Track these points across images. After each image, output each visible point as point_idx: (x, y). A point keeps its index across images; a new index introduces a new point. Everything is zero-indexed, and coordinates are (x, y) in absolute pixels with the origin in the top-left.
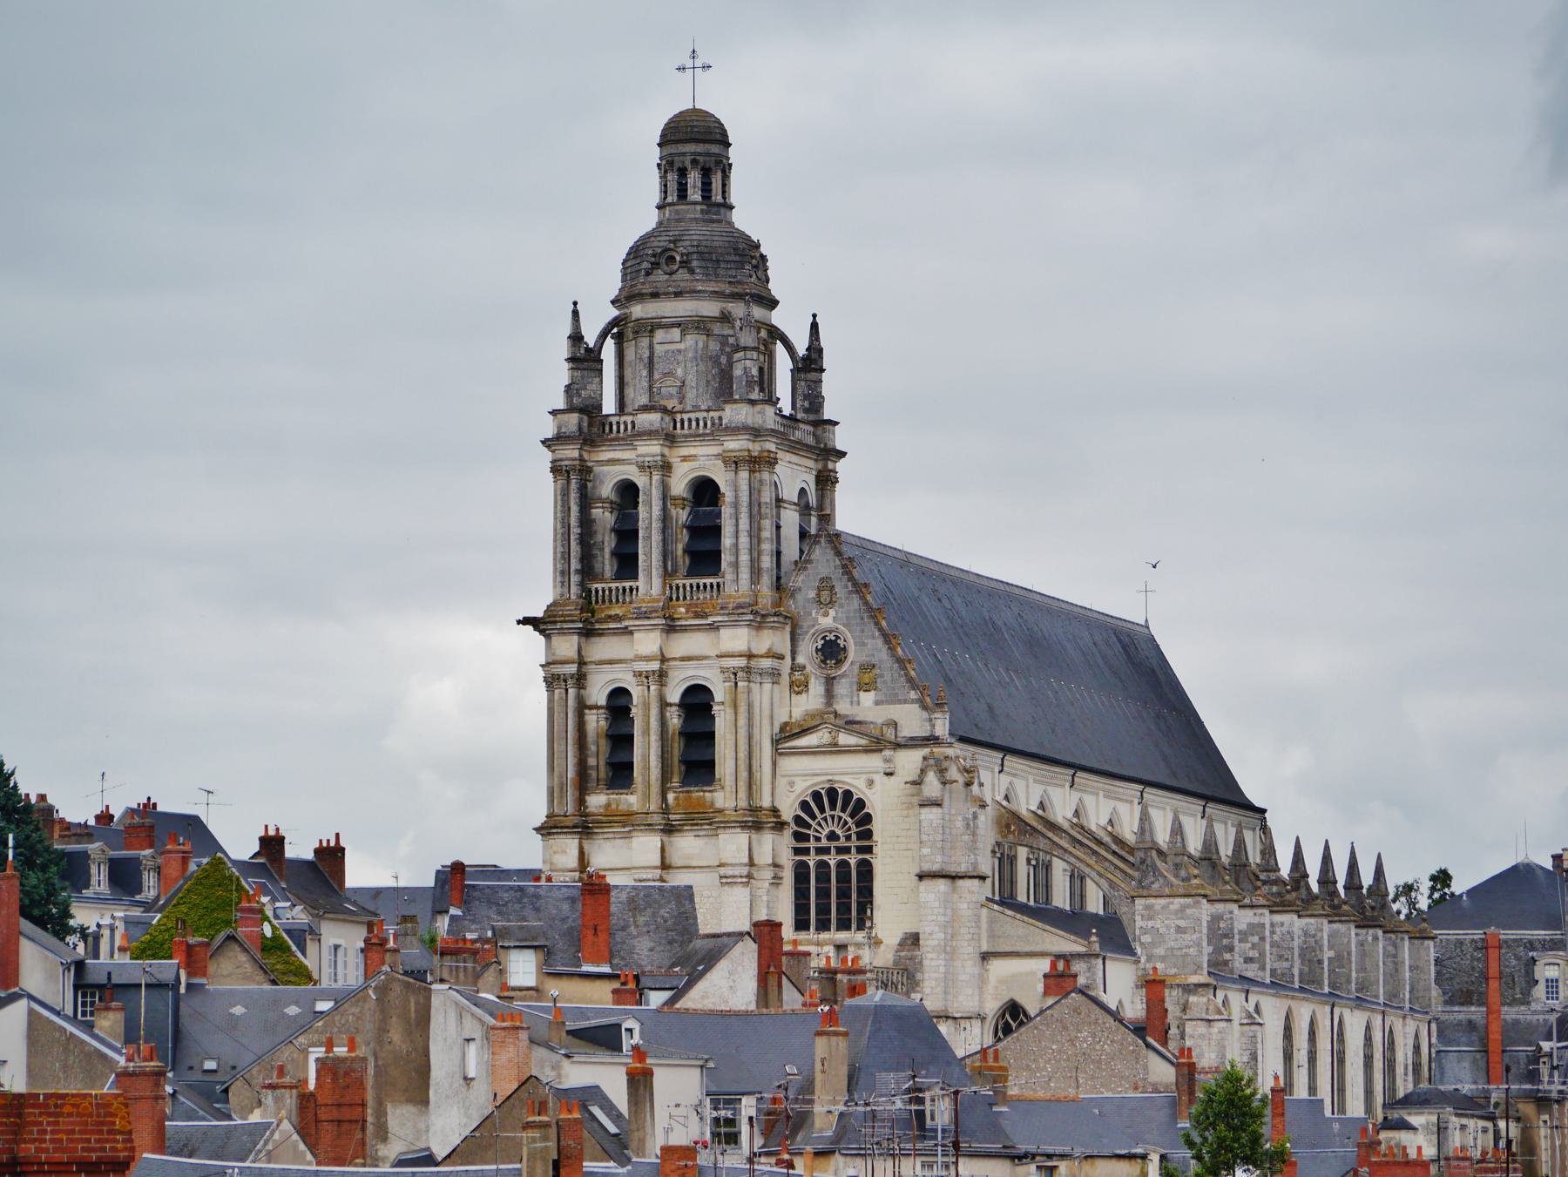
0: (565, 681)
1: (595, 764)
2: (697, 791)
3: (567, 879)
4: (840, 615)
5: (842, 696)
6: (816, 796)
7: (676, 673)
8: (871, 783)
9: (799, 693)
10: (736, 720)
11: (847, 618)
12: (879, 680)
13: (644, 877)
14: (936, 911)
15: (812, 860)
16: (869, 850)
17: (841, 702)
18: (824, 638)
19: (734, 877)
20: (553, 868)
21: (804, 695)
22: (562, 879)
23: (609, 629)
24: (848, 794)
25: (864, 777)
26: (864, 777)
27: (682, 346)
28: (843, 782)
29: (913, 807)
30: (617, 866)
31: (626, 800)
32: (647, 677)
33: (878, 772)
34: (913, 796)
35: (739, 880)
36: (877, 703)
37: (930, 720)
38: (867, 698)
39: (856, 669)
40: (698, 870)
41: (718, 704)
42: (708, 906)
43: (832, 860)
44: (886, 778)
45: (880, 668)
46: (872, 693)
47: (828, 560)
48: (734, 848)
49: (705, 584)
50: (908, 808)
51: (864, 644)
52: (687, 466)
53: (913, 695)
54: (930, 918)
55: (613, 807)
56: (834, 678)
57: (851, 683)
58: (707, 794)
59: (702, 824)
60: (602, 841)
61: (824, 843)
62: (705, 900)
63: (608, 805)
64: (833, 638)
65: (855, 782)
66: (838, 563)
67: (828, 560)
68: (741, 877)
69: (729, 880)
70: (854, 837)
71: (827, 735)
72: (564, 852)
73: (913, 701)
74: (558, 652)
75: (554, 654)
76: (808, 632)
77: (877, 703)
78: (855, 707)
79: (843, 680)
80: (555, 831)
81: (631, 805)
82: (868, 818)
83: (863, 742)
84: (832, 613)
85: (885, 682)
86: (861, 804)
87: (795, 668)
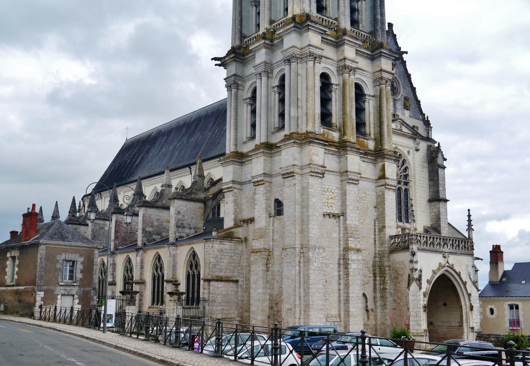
0: (315, 58)
2: (362, 138)
3: (320, 171)
5: (399, 109)
8: (409, 152)
10: (307, 110)
11: (399, 74)
13: (353, 177)
16: (406, 184)
17: (399, 112)
19: (391, 185)
20: (312, 163)
22: (317, 170)
23: (327, 39)
25: (407, 149)
28: (399, 150)
29: (424, 168)
30: (330, 170)
32: (350, 70)
33: (412, 149)
34: (424, 162)
35: (393, 188)
36: (410, 117)
38: (407, 113)
39: (403, 98)
40: (365, 179)
41: (369, 96)
42: (368, 199)
44: (415, 152)
45: (410, 101)
46: (408, 111)
47: (393, 45)
50: (423, 168)
53: (421, 117)
55: (326, 136)
56: (396, 100)
57: (402, 104)
58: (365, 140)
59: (368, 155)
65: (404, 151)
67: (393, 45)
68: (394, 186)
69: (390, 187)
70: (402, 177)
71: (399, 125)
72: (318, 155)
75: (310, 41)
77: (410, 117)
78: (403, 116)
79: (399, 102)
81: (333, 137)
82: (406, 169)
83: (410, 132)
85: (412, 108)
86: (404, 162)
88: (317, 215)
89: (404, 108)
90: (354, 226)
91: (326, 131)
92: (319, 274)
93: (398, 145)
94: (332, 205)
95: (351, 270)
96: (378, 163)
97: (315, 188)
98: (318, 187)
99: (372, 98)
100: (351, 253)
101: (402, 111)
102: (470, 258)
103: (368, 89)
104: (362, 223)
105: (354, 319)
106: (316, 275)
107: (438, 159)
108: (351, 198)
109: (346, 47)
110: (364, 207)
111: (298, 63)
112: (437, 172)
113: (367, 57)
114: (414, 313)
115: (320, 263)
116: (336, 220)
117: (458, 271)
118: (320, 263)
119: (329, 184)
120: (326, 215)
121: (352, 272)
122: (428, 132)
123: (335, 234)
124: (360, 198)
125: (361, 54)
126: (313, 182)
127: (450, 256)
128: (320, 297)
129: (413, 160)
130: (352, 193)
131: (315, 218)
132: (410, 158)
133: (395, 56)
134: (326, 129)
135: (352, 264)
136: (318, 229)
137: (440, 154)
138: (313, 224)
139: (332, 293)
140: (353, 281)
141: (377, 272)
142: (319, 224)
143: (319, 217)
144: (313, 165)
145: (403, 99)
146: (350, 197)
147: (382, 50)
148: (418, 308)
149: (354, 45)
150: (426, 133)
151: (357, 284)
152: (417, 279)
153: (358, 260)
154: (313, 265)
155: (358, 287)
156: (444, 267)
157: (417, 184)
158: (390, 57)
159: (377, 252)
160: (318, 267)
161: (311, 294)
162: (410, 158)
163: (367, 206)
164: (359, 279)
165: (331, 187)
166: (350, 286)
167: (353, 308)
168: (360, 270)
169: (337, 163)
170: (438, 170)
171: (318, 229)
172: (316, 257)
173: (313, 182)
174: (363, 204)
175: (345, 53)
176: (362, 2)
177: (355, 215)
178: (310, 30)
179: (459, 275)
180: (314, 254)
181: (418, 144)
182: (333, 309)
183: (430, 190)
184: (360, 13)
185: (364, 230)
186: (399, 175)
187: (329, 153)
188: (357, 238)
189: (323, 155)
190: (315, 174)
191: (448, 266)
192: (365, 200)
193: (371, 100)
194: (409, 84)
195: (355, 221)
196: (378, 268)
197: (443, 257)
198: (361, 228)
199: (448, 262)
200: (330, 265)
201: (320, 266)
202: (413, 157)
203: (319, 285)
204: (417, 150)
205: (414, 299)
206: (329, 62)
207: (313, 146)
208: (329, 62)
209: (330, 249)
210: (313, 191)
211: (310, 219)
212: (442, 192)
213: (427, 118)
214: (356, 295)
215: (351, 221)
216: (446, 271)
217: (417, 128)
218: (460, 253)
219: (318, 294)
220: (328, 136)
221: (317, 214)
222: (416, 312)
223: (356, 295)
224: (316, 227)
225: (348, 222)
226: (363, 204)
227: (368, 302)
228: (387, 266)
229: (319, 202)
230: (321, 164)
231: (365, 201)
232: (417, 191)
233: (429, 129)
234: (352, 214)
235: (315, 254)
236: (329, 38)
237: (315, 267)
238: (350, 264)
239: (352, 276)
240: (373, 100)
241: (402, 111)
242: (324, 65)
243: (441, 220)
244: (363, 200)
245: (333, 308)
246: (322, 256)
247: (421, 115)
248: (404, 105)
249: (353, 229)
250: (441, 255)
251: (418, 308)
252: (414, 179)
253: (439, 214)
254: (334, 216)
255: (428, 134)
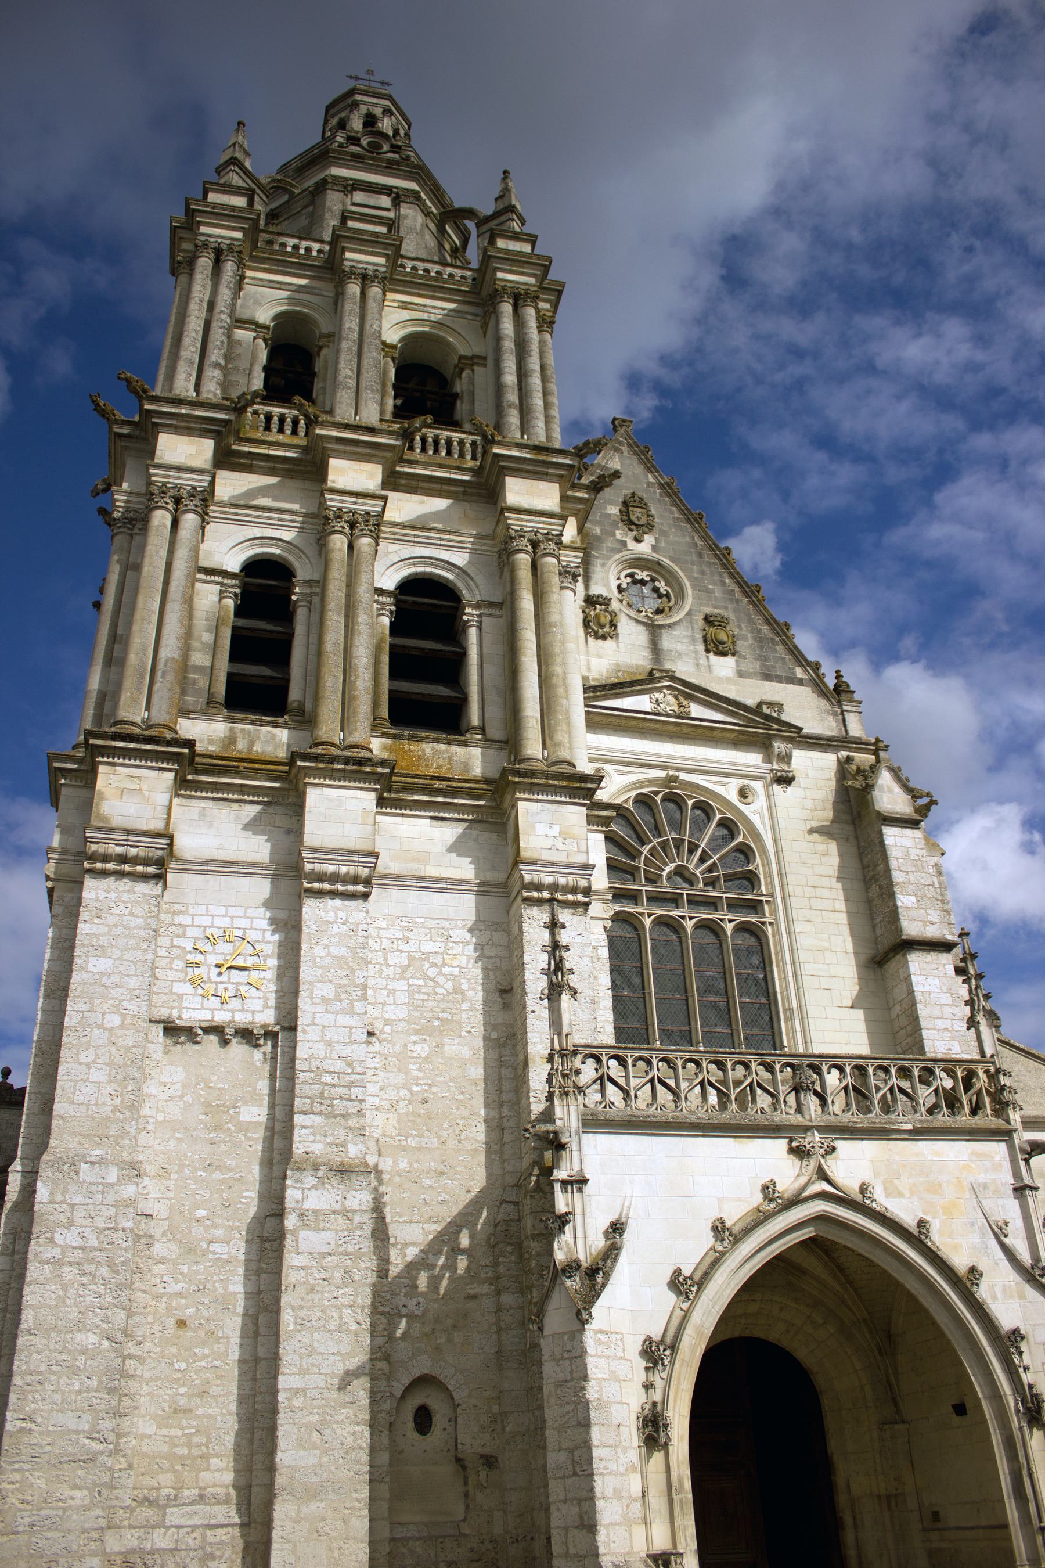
1: (208, 664)
4: (663, 545)
5: (680, 654)
6: (644, 801)
7: (393, 547)
9: (604, 637)
12: (739, 643)
14: (948, 1011)
15: (648, 915)
18: (631, 575)
21: (609, 643)
24: (704, 808)
25: (735, 784)
26: (735, 784)
27: (391, 215)
31: (274, 735)
33: (761, 778)
37: (834, 714)
39: (699, 619)
43: (689, 919)
44: (776, 788)
46: (730, 660)
48: (555, 831)
49: (449, 442)
51: (707, 591)
52: (406, 315)
53: (799, 673)
54: (940, 1024)
57: (693, 640)
60: (209, 804)
61: (666, 887)
62: (457, 949)
63: (231, 740)
64: (648, 579)
66: (651, 479)
68: (574, 890)
71: (671, 699)
73: (800, 682)
74: (166, 458)
75: (161, 458)
76: (611, 557)
77: (741, 674)
80: (122, 744)
84: (649, 539)
87: (590, 601)
88: (108, 1025)
89: (707, 651)
90: (340, 1066)
91: (243, 730)
92: (85, 1280)
93: (677, 769)
94: (243, 989)
95: (292, 1259)
96: (508, 818)
97: (112, 920)
98: (131, 914)
99: (494, 611)
100: (297, 1181)
101: (697, 659)
102: (998, 1150)
103: (477, 587)
104: (426, 1058)
105: (305, 1510)
106: (64, 1287)
107: (876, 793)
108: (329, 954)
109: (334, 463)
110: (436, 994)
111: (131, 535)
112: (882, 843)
113: (464, 493)
114: (562, 1456)
115: (100, 1231)
116: (262, 1049)
117: (909, 1221)
118: (100, 1231)
119: (232, 911)
120: (207, 1030)
121: (303, 1268)
122: (844, 720)
123: (255, 1110)
124: (411, 958)
125: (438, 486)
126: (102, 895)
127: (840, 1144)
128: (80, 1392)
129: (772, 819)
130: (335, 929)
131: (98, 1036)
132: (755, 813)
133: (560, 460)
134: (242, 721)
135: (303, 1234)
136: (110, 1082)
137: (885, 779)
138: (83, 1058)
139: (219, 1377)
140: (303, 1313)
141: (501, 1269)
142: (119, 1060)
143: (120, 1032)
144: (100, 829)
145: (700, 623)
146: (319, 951)
147: (496, 450)
148: (579, 1424)
149: (368, 451)
150: (834, 724)
151: (333, 1325)
152: (572, 1267)
153: (346, 1213)
154: (51, 1240)
155: (339, 1342)
156: (795, 1201)
157: (794, 902)
158: (545, 470)
159: (510, 1180)
160: (83, 1249)
161: (17, 1380)
162: (755, 813)
163: (457, 990)
164: (345, 1301)
165: (244, 923)
166: (282, 1337)
167: (300, 1446)
168: (357, 1256)
169: (289, 832)
170: (881, 834)
171: (110, 1082)
172: (73, 1206)
173: (102, 895)
174: (431, 980)
175: (330, 477)
176: (473, 371)
177: (345, 1020)
178: (160, 428)
179: (917, 1238)
180: (65, 1192)
181: (786, 758)
182: (214, 1462)
183: (871, 916)
184: (466, 398)
185: (434, 1089)
186: (697, 872)
187: (245, 801)
188: (345, 1116)
189: (167, 796)
190: (110, 866)
191: (822, 1195)
192: (445, 964)
193: (489, 615)
194: (725, 575)
195: (346, 1044)
196: (509, 1249)
197: (792, 1150)
198: (418, 1078)
199: (822, 1175)
200: (215, 1247)
201: (94, 1243)
202: (770, 808)
203: (79, 1337)
204: (785, 780)
205: (561, 1376)
206: (279, 519)
207: (114, 764)
208: (279, 519)
209: (218, 1176)
210: (103, 930)
211: (65, 1039)
212: (913, 913)
213: (838, 676)
214: (322, 1384)
215: (321, 1046)
216: (822, 1219)
217: (779, 706)
218: (909, 1127)
219: (64, 1380)
220: (252, 743)
221: (115, 1020)
222: (571, 1451)
223: (322, 1384)
224: (98, 1075)
225: (301, 1052)
226: (431, 980)
227: (460, 1420)
228: (534, 1237)
229: (132, 972)
230: (158, 825)
231: (446, 970)
232: (798, 927)
233: (845, 708)
234: (331, 1016)
235: (72, 1188)
236: (272, 452)
237: (65, 1248)
238: (294, 1232)
239: (301, 1290)
240: (500, 617)
241: (697, 659)
242: (258, 532)
243: (923, 1023)
244: (433, 965)
245: (216, 1455)
246: (110, 1198)
247: (801, 665)
248: (705, 641)
249: (327, 1079)
250: (780, 1145)
251: (579, 1424)
252: (782, 886)
253: (914, 1004)
254: (246, 1035)
255: (845, 726)
